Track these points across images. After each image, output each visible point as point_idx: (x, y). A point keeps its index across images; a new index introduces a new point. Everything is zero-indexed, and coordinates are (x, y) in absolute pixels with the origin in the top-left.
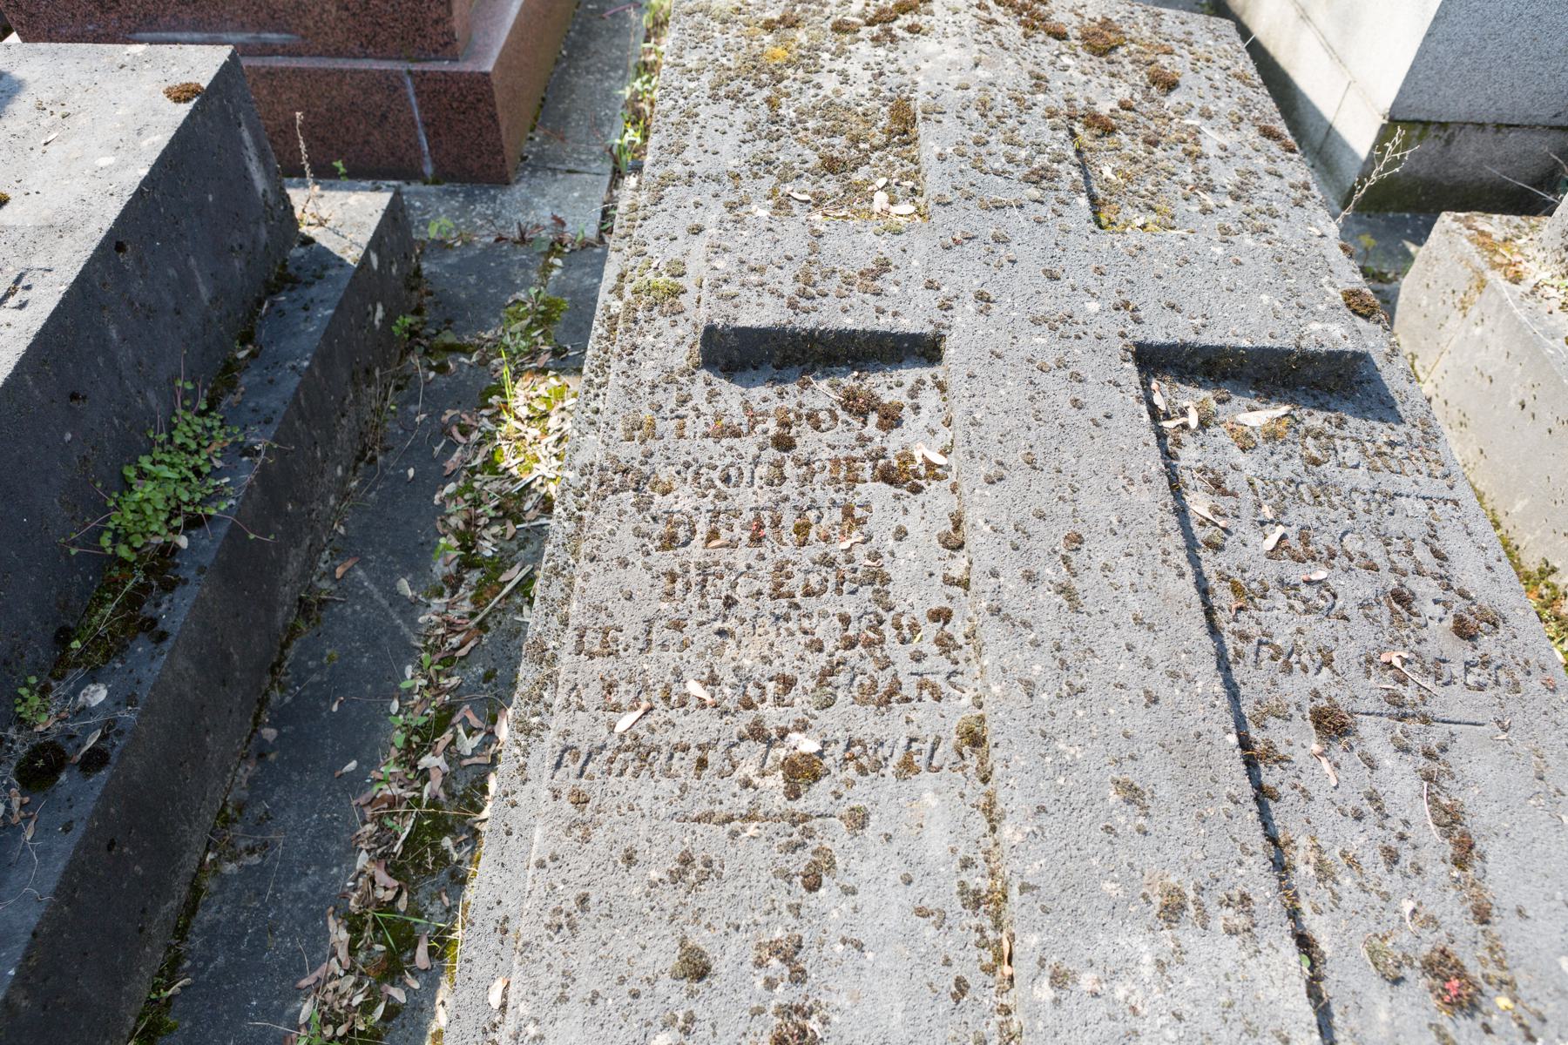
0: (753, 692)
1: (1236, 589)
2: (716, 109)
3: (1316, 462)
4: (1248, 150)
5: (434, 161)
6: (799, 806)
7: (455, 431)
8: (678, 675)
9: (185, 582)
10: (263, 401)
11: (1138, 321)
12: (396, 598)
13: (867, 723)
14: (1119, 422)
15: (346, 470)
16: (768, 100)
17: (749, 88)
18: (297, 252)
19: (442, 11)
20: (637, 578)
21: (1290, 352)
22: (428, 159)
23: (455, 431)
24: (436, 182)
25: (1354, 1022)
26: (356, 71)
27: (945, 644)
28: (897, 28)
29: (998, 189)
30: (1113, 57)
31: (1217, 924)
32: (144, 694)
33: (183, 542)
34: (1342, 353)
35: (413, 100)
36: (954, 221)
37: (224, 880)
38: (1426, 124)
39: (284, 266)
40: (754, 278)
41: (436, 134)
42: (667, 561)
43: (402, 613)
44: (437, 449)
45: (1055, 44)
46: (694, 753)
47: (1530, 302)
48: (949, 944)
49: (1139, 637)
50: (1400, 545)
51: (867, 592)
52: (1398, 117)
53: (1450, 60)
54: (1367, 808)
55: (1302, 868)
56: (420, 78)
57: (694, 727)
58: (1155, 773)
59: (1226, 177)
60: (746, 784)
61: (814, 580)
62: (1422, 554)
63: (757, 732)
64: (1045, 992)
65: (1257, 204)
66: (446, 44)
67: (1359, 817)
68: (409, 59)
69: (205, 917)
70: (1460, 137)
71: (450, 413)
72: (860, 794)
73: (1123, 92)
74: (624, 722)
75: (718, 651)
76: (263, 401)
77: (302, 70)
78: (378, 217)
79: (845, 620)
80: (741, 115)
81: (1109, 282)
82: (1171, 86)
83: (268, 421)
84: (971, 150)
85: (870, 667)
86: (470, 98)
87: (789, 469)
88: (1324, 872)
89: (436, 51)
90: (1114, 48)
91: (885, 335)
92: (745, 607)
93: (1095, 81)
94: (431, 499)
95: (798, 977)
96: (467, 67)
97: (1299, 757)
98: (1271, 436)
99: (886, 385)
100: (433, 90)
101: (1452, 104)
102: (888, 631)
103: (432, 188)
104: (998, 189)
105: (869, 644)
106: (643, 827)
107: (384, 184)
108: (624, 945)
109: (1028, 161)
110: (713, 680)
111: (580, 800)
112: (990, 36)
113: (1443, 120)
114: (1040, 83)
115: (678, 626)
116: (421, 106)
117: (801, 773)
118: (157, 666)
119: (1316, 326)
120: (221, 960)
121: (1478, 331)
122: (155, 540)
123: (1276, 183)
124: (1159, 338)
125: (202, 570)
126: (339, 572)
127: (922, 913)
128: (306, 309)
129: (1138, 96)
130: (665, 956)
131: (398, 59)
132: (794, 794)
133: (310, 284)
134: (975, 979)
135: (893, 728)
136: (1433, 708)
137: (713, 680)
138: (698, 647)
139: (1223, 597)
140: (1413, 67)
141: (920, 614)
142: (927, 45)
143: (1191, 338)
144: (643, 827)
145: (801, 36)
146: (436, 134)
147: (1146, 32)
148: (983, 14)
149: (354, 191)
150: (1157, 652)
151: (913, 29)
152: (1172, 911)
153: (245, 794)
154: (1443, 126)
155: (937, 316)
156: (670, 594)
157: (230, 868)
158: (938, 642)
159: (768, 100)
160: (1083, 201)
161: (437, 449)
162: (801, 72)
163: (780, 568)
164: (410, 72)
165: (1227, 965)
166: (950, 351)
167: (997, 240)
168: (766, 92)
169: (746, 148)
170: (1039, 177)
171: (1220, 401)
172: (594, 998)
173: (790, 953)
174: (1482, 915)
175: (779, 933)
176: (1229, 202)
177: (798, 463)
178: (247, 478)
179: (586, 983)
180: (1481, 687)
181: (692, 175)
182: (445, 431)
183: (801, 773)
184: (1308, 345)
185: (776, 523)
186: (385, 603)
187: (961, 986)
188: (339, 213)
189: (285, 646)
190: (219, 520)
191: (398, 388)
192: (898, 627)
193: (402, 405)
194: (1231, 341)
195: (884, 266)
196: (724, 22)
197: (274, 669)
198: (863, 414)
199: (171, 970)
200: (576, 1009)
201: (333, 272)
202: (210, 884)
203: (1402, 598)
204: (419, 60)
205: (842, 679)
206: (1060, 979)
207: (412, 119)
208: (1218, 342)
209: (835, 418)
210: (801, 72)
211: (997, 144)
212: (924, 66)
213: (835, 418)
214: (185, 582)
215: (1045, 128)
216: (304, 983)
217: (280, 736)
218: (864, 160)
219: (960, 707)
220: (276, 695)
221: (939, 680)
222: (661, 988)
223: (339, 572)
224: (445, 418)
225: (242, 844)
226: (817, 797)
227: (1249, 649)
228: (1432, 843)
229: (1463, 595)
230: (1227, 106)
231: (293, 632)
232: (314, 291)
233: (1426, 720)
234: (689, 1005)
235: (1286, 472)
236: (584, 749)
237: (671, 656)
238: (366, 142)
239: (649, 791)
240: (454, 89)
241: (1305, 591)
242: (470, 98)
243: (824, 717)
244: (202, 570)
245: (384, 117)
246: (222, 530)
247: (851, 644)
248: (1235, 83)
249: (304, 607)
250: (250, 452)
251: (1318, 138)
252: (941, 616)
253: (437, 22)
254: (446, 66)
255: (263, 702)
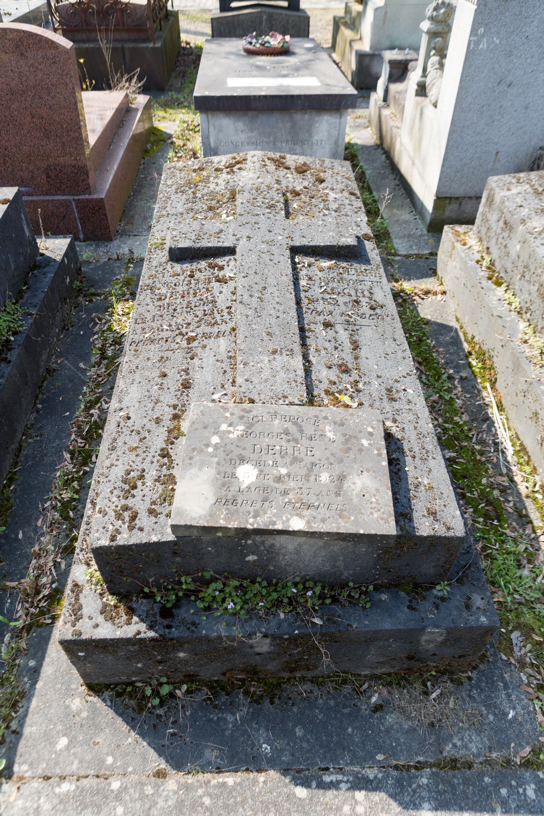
0: (180, 327)
1: (309, 299)
2: (176, 196)
3: (341, 274)
4: (344, 198)
5: (83, 233)
6: (190, 346)
7: (97, 320)
8: (161, 325)
9: (14, 348)
10: (33, 301)
11: (292, 240)
12: (79, 369)
13: (208, 329)
14: (282, 263)
15: (59, 330)
16: (193, 192)
17: (187, 189)
18: (39, 258)
19: (85, 176)
20: (151, 307)
21: (335, 246)
22: (81, 232)
23: (97, 320)
24: (84, 241)
25: (317, 374)
26: (54, 200)
27: (229, 313)
28: (235, 169)
29: (258, 211)
30: (305, 174)
31: (284, 354)
32: (6, 375)
33: (12, 339)
34: (350, 245)
35: (75, 210)
36: (244, 219)
37: (29, 444)
38: (451, 198)
39: (35, 262)
40: (184, 236)
41: (84, 222)
42: (160, 303)
43: (81, 373)
44: (91, 325)
45: (286, 171)
46: (165, 339)
47: (467, 251)
48: (223, 365)
49: (277, 306)
50: (360, 291)
51: (211, 305)
52: (440, 196)
53: (453, 174)
54: (333, 340)
55: (312, 350)
56: (78, 201)
57: (164, 335)
58: (276, 330)
59: (334, 206)
60: (177, 343)
61: (197, 304)
62: (367, 293)
63: (181, 334)
64: (242, 366)
65: (342, 213)
66: (87, 189)
67: (330, 341)
68: (73, 195)
69: (24, 453)
70: (464, 202)
71: (94, 314)
72: (205, 342)
73: (306, 184)
74: (147, 335)
75: (172, 320)
76: (33, 301)
77: (34, 201)
78: (66, 246)
79: (205, 311)
80: (184, 196)
81: (286, 232)
82: (322, 181)
83: (35, 306)
84: (251, 201)
85: (210, 319)
86: (97, 208)
87: (193, 282)
88: (317, 350)
89: (83, 192)
90: (305, 171)
91: (220, 247)
92: (179, 310)
93: (297, 181)
94: (89, 340)
95: (188, 374)
96: (95, 196)
97: (317, 331)
98: (329, 268)
99: (220, 261)
100: (82, 206)
101: (459, 191)
102: (215, 312)
103: (83, 244)
104: (258, 211)
105: (210, 315)
106: (152, 354)
107: (68, 236)
108: (147, 373)
109: (268, 203)
110: (170, 325)
111: (136, 351)
112: (264, 169)
113: (456, 196)
114: (278, 182)
115: (162, 316)
116: (78, 212)
117: (190, 340)
118: (9, 369)
119: (344, 239)
120: (30, 463)
121: (454, 263)
122: (3, 338)
123: (350, 207)
124: (297, 244)
125: (19, 345)
126: (59, 362)
127: (217, 361)
128: (44, 274)
129: (310, 185)
130: (158, 373)
131: (69, 195)
132: (189, 343)
133: (44, 267)
134: (228, 370)
135: (215, 330)
136: (358, 323)
137: (170, 325)
138: (167, 319)
139: (305, 301)
140: (440, 178)
141: (224, 308)
142: (244, 173)
143: (307, 244)
144: (152, 354)
145: (205, 173)
146: (84, 222)
147: (318, 166)
148: (263, 163)
149: (57, 238)
150: (281, 309)
151: (240, 169)
152: (275, 352)
153: (33, 422)
154: (457, 198)
155: (235, 242)
156: (160, 310)
157: (30, 441)
158: (228, 312)
159: (193, 192)
160: (283, 212)
161: (91, 325)
162: (204, 184)
163: (188, 302)
164: (74, 199)
165: (285, 360)
166: (238, 250)
167: (255, 223)
168: (192, 190)
169: (185, 206)
170: (271, 207)
171: (316, 261)
172: (140, 383)
173: (186, 371)
174: (356, 358)
175: (184, 368)
176: (333, 213)
177: (195, 280)
178: (30, 321)
179: (137, 381)
180: (373, 319)
181: (168, 214)
182: (93, 320)
183: (190, 340)
184: (341, 244)
185: (188, 293)
186: (75, 370)
187: (225, 371)
188: (52, 246)
189: (43, 382)
190: (23, 333)
191: (75, 307)
192: (218, 311)
193: (77, 313)
194: (318, 244)
195: (221, 231)
196: (180, 170)
197: (40, 387)
198: (213, 268)
199: (15, 464)
200: (135, 385)
201: (52, 263)
202: (25, 445)
203: (357, 302)
204: (77, 195)
205: (203, 322)
206: (245, 364)
207: (75, 217)
208: (314, 244)
209: (206, 269)
210: (204, 184)
211: (260, 199)
212: (242, 179)
213: (206, 269)
214: (14, 348)
215: (275, 194)
216: (57, 468)
217: (43, 407)
218: (221, 206)
219: (231, 325)
220: (40, 396)
221: (228, 320)
222: (156, 379)
223: (59, 362)
224: (93, 316)
225: (34, 435)
226: (195, 344)
227: (310, 311)
228: (348, 346)
229: (375, 301)
230: (340, 186)
231: (45, 379)
232: (46, 269)
233: (355, 325)
234: (163, 381)
235: (331, 275)
236: (137, 341)
237: (159, 322)
238: (58, 227)
239: (152, 347)
240: (90, 205)
241: (329, 300)
242: (97, 208)
243: (197, 329)
244: (19, 345)
245: (64, 217)
246: (24, 335)
247: (205, 315)
248: (345, 180)
249: (49, 371)
250: (31, 314)
251: (420, 207)
252: (229, 308)
253: (83, 181)
254: (87, 197)
255: (37, 397)
